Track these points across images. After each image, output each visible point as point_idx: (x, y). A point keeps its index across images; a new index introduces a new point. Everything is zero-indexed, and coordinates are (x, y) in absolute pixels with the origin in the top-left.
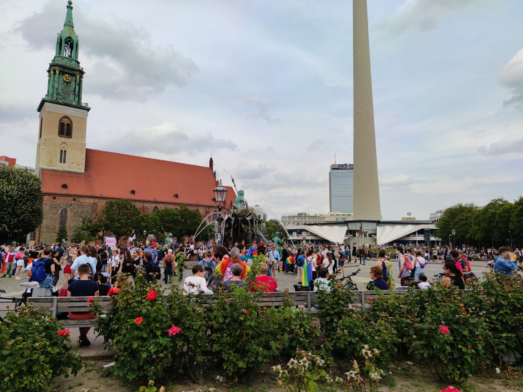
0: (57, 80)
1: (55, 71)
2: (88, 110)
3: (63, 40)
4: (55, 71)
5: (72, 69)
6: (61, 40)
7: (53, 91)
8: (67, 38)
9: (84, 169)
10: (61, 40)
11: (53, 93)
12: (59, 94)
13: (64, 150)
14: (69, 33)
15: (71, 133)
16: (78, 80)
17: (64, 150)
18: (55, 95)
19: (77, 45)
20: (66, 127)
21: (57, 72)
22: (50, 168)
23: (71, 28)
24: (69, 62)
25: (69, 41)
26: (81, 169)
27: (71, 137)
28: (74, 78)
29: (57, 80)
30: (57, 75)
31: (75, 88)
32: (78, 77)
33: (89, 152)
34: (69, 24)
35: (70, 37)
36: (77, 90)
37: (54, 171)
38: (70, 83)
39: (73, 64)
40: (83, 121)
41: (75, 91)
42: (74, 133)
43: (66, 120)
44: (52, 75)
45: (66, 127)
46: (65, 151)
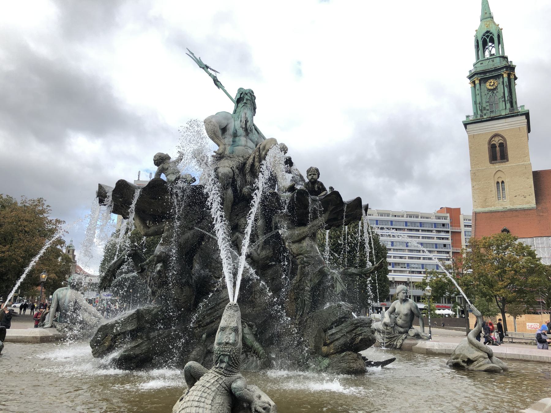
0: (477, 92)
2: (527, 115)
4: (474, 82)
5: (496, 70)
6: (477, 42)
8: (484, 35)
10: (478, 41)
12: (485, 108)
13: (500, 181)
16: (506, 79)
17: (500, 181)
18: (479, 112)
19: (499, 36)
20: (498, 149)
21: (477, 82)
22: (486, 209)
23: (489, 19)
24: (491, 63)
25: (488, 36)
30: (478, 86)
33: (537, 175)
34: (487, 16)
35: (488, 32)
36: (506, 94)
37: (491, 212)
39: (498, 63)
42: (511, 153)
43: (497, 139)
45: (498, 149)
46: (503, 182)
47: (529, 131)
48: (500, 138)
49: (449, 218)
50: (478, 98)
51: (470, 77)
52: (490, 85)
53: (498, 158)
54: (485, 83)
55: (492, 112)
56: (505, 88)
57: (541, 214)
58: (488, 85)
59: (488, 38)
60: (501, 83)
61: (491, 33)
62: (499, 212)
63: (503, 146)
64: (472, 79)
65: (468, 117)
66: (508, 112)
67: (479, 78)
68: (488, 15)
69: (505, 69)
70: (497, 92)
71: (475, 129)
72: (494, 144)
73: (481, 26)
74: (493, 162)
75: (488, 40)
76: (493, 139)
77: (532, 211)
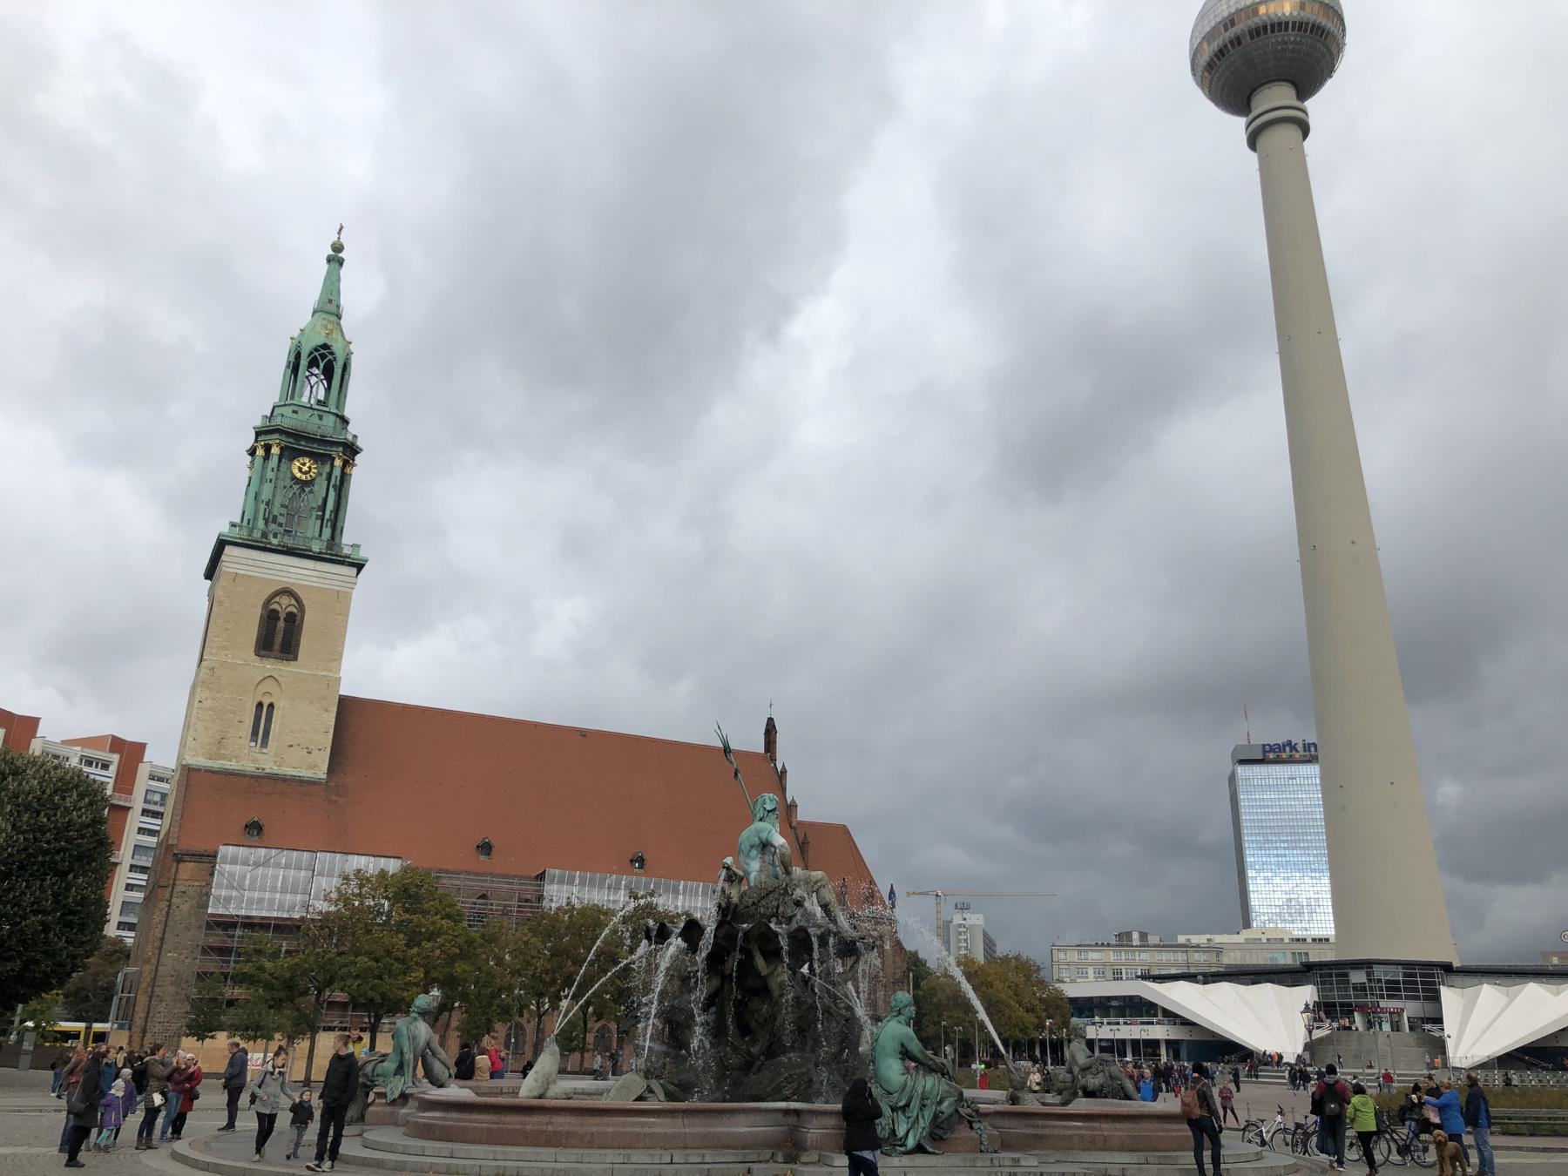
0: (270, 475)
1: (268, 448)
2: (359, 567)
3: (304, 355)
4: (268, 448)
5: (323, 441)
7: (256, 512)
11: (255, 518)
12: (275, 517)
14: (323, 333)
16: (337, 472)
18: (261, 524)
19: (345, 367)
20: (281, 624)
21: (275, 450)
23: (334, 318)
24: (316, 420)
25: (323, 357)
26: (317, 767)
28: (327, 468)
29: (270, 475)
30: (274, 461)
31: (325, 500)
32: (338, 463)
33: (347, 706)
34: (329, 307)
35: (325, 346)
36: (330, 506)
39: (328, 425)
40: (339, 603)
41: (323, 508)
44: (259, 461)
45: (281, 624)
46: (271, 706)
49: (113, 769)
51: (258, 434)
52: (300, 470)
53: (277, 647)
54: (292, 460)
58: (301, 467)
59: (321, 361)
62: (244, 776)
63: (294, 622)
68: (332, 308)
72: (276, 611)
73: (312, 325)
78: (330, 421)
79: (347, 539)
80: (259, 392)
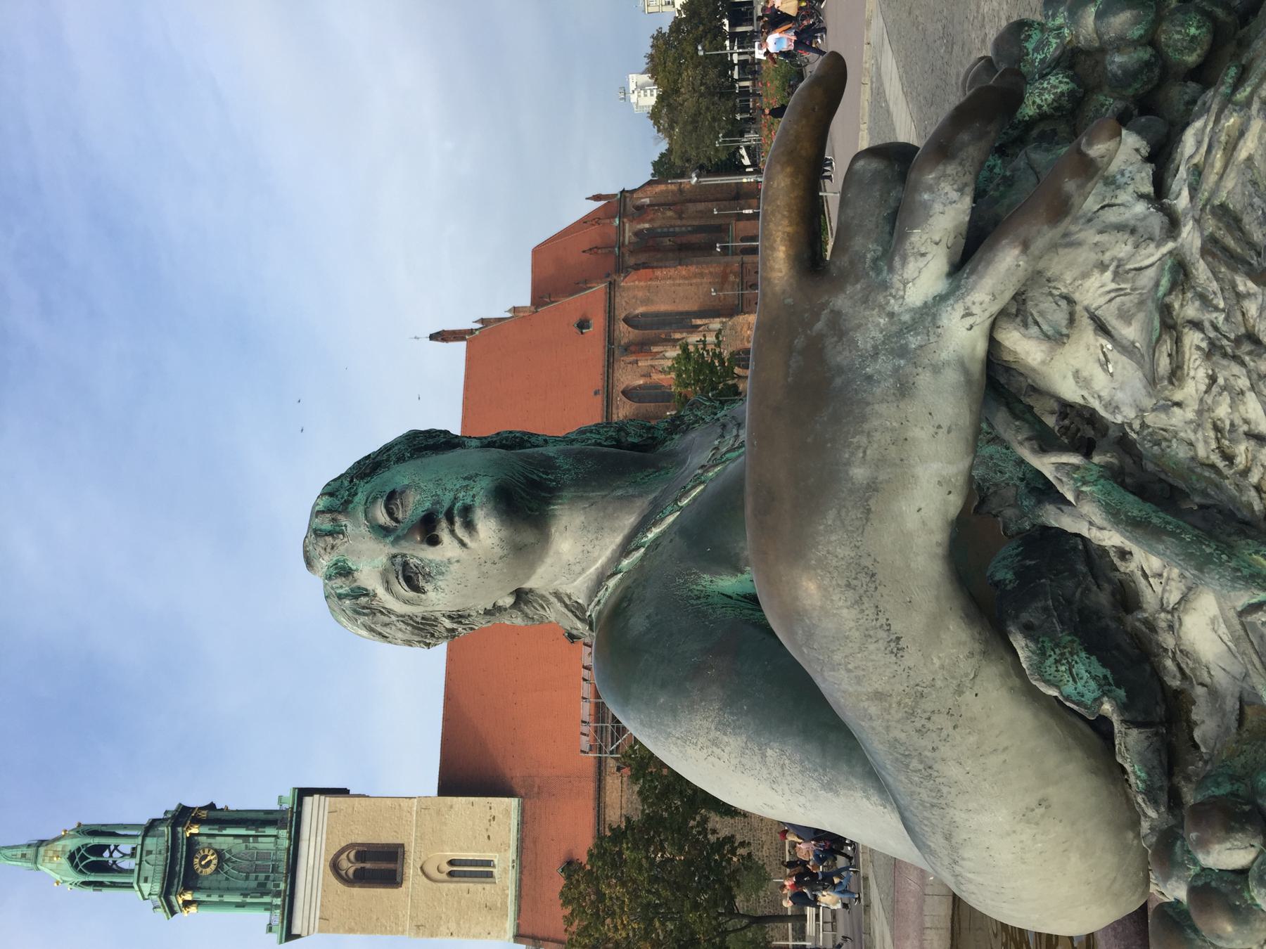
0: (215, 898)
2: (303, 793)
4: (187, 904)
5: (173, 848)
8: (76, 867)
9: (506, 800)
15: (388, 845)
16: (205, 830)
18: (267, 899)
19: (94, 832)
20: (368, 865)
21: (188, 897)
24: (151, 858)
25: (83, 858)
27: (402, 846)
28: (203, 839)
29: (215, 898)
32: (195, 830)
35: (72, 858)
37: (519, 897)
38: (219, 854)
42: (385, 836)
45: (368, 865)
46: (451, 863)
47: (343, 792)
48: (344, 856)
50: (227, 898)
53: (391, 866)
55: (275, 869)
56: (224, 832)
57: (536, 790)
60: (210, 840)
61: (79, 849)
63: (365, 853)
64: (177, 908)
65: (270, 929)
66: (284, 833)
67: (181, 889)
69: (180, 829)
70: (229, 851)
71: (307, 913)
72: (356, 871)
74: (398, 879)
75: (93, 859)
76: (343, 873)
77: (527, 807)
78: (151, 843)
79: (274, 806)
80: (133, 907)
